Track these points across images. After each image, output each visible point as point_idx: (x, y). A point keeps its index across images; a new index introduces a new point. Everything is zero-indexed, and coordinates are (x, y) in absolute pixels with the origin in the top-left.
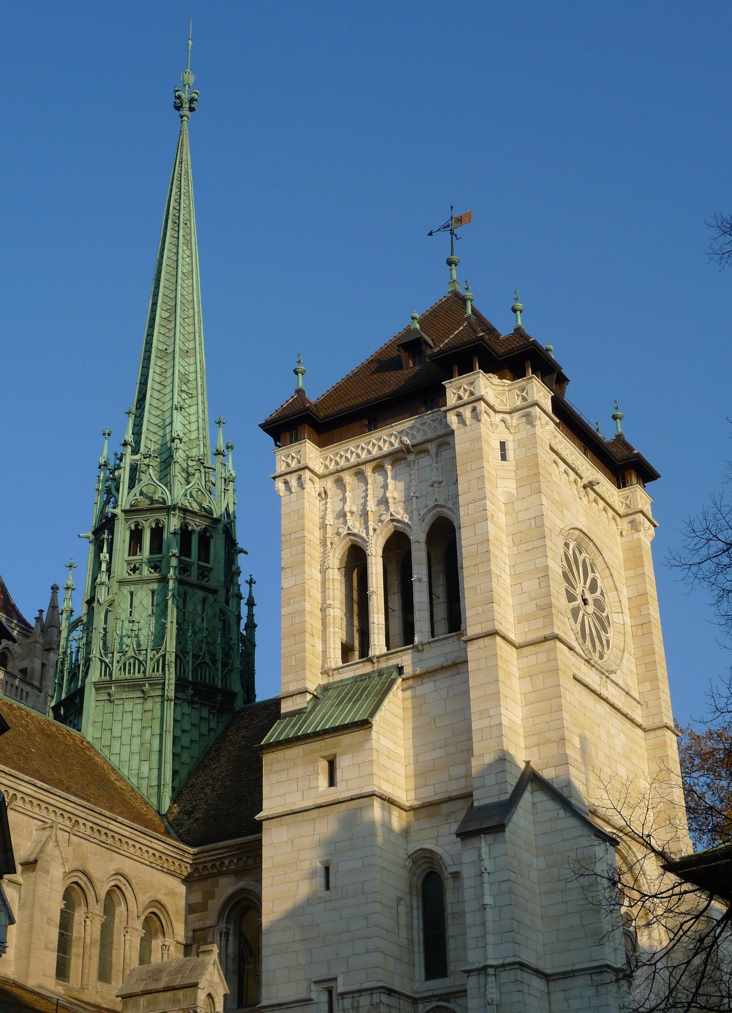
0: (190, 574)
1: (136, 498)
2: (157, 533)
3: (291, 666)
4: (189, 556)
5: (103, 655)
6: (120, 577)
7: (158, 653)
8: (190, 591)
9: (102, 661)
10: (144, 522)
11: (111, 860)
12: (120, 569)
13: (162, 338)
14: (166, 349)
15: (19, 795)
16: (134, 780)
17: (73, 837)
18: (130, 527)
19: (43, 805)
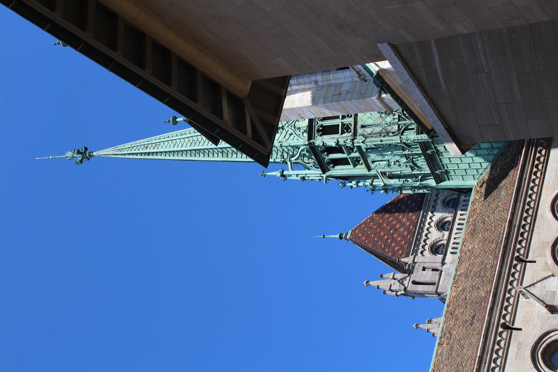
0: (349, 124)
1: (313, 166)
2: (330, 150)
3: (366, 107)
4: (339, 125)
5: (417, 179)
6: (366, 170)
7: (404, 147)
8: (359, 124)
9: (421, 180)
10: (326, 160)
11: (542, 216)
12: (361, 170)
13: (216, 155)
14: (221, 152)
15: (502, 321)
16: (495, 152)
17: (529, 259)
18: (332, 167)
19: (508, 295)
